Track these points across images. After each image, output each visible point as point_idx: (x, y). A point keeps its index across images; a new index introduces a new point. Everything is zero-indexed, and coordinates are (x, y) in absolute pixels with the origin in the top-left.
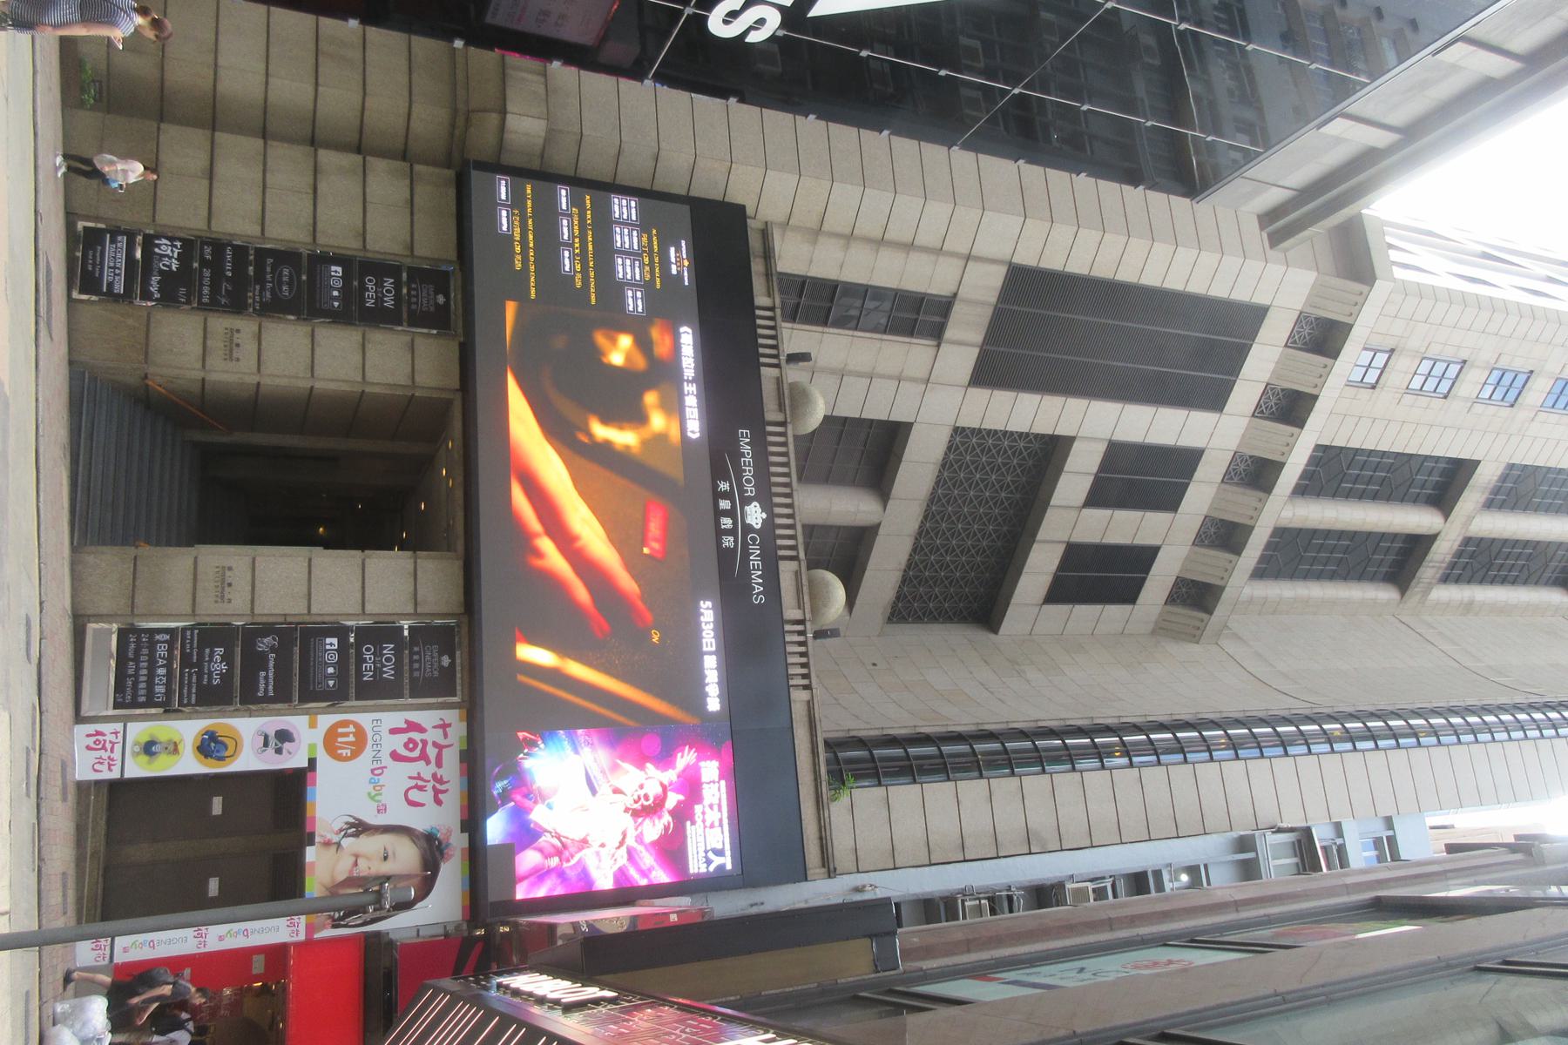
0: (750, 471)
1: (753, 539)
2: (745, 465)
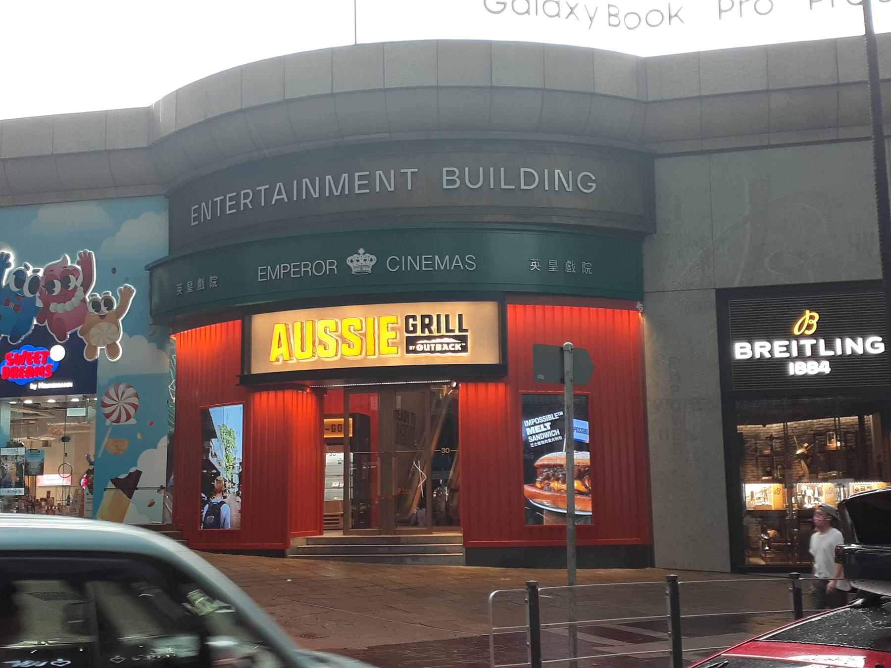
0: (306, 266)
1: (393, 263)
2: (299, 272)
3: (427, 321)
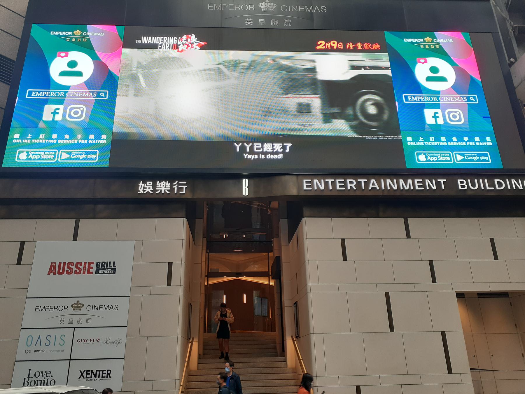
3: (103, 264)
